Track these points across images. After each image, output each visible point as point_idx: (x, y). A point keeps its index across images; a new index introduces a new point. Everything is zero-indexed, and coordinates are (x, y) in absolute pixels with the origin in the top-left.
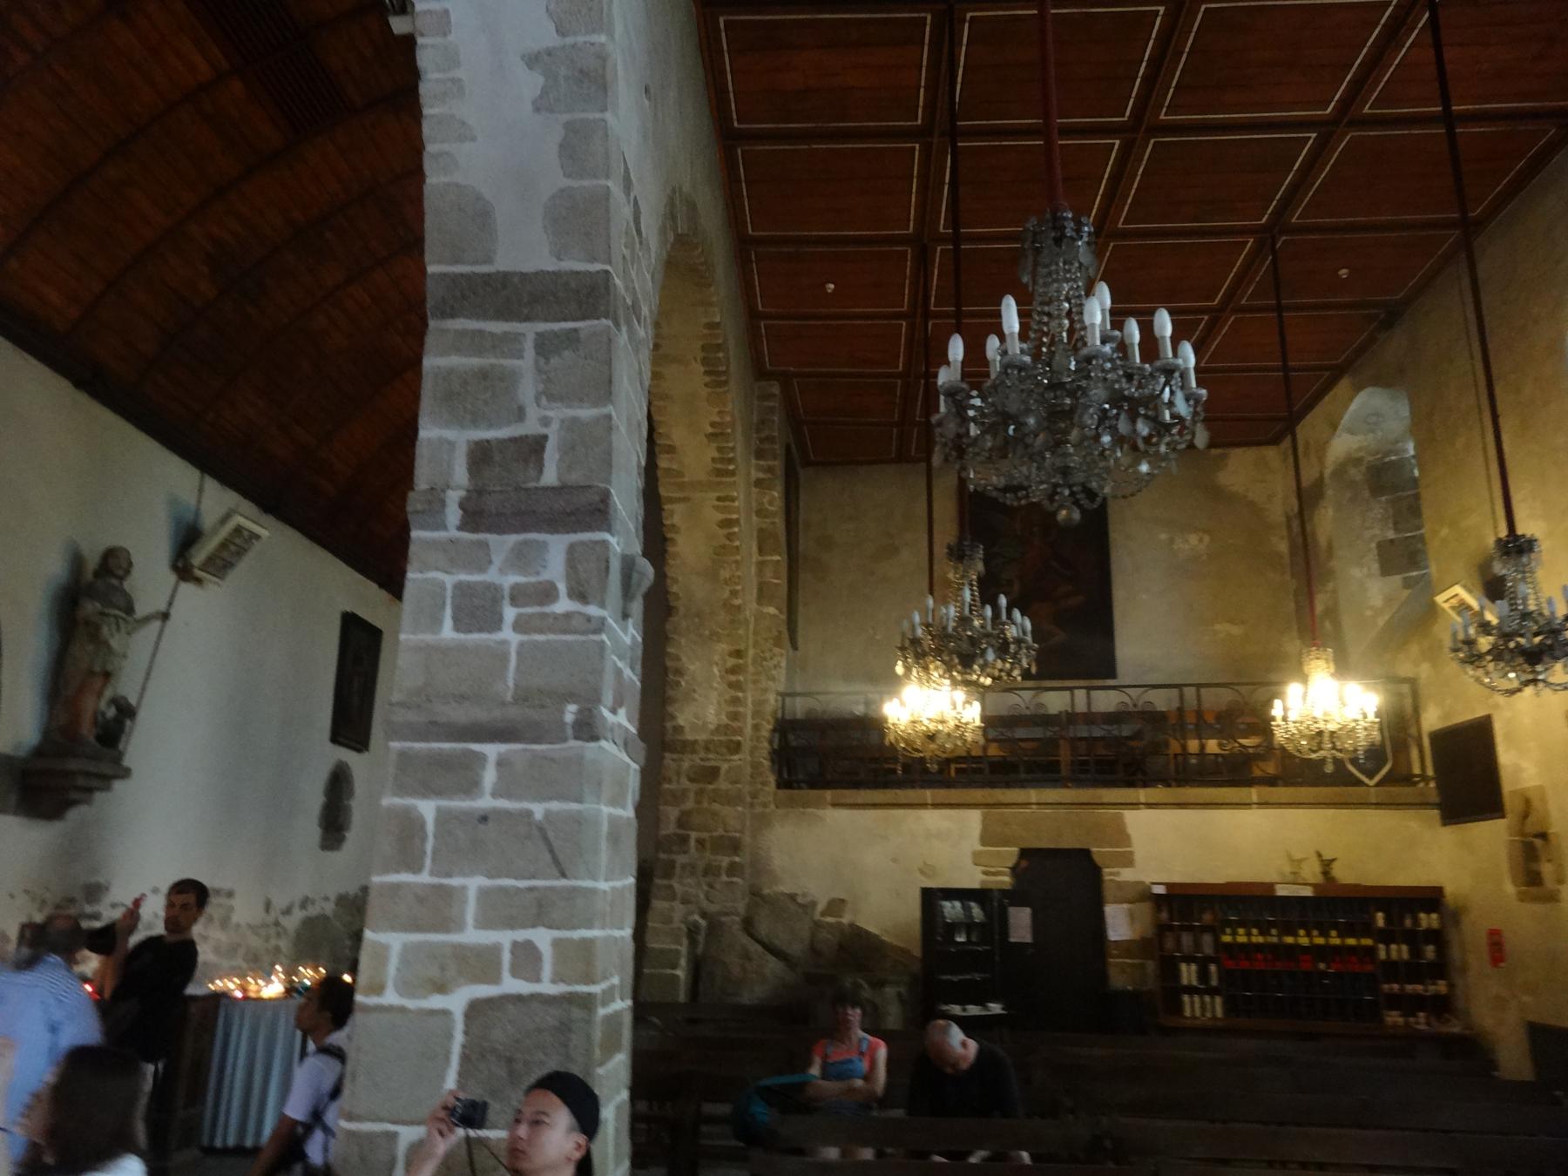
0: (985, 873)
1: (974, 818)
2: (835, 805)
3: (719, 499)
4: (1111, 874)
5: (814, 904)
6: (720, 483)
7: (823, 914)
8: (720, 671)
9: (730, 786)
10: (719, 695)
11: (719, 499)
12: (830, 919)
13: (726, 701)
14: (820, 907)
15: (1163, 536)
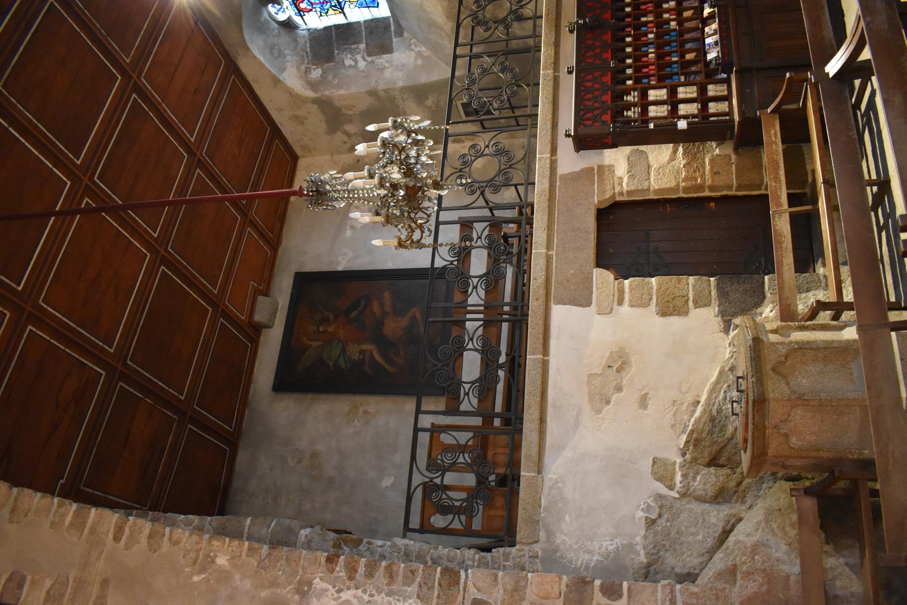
0: (620, 302)
1: (559, 312)
2: (539, 469)
3: (117, 538)
4: (621, 184)
5: (659, 497)
6: (93, 531)
7: (671, 488)
8: (349, 588)
9: (500, 586)
10: (379, 593)
11: (117, 538)
12: (678, 478)
13: (388, 584)
14: (662, 489)
15: (349, 233)
